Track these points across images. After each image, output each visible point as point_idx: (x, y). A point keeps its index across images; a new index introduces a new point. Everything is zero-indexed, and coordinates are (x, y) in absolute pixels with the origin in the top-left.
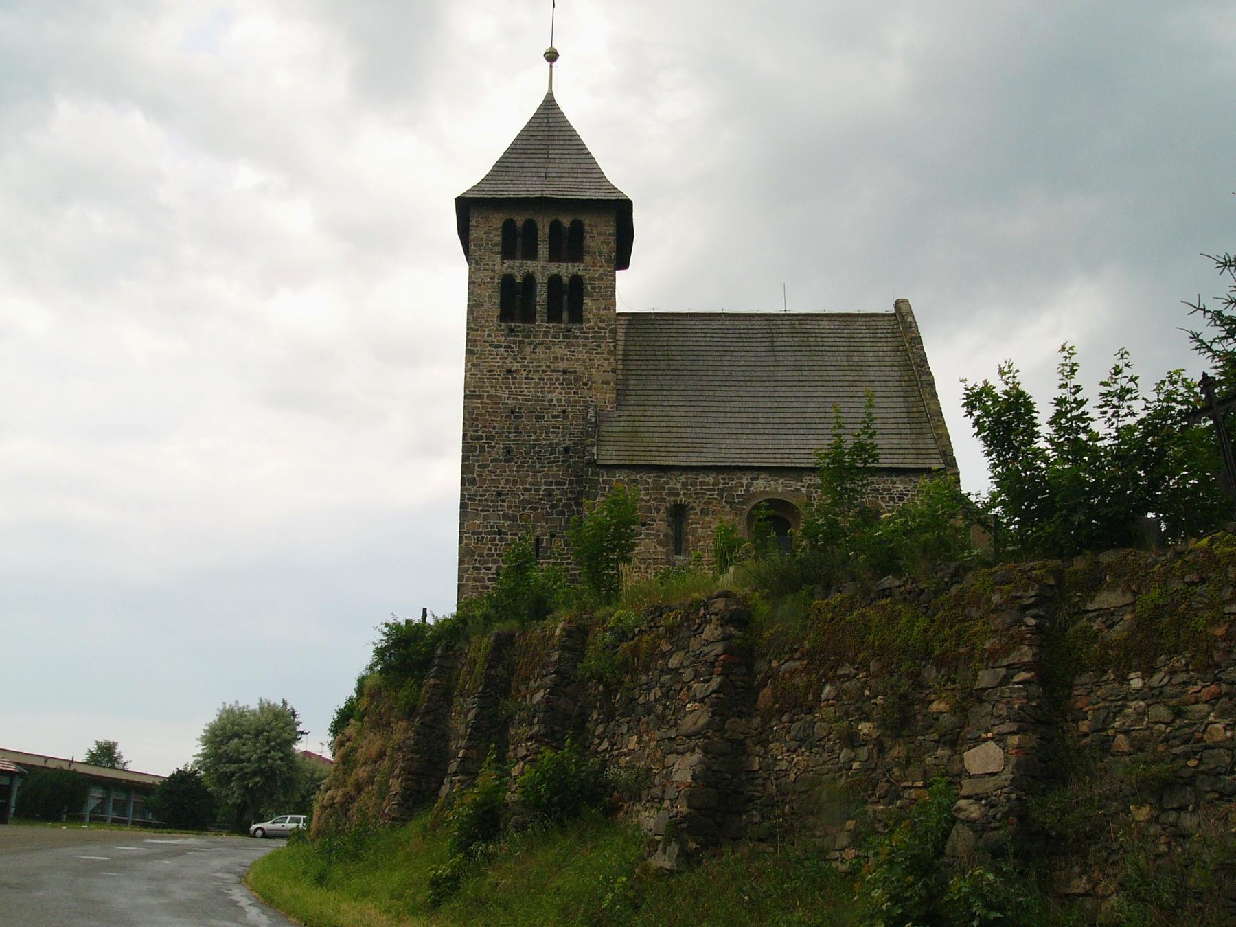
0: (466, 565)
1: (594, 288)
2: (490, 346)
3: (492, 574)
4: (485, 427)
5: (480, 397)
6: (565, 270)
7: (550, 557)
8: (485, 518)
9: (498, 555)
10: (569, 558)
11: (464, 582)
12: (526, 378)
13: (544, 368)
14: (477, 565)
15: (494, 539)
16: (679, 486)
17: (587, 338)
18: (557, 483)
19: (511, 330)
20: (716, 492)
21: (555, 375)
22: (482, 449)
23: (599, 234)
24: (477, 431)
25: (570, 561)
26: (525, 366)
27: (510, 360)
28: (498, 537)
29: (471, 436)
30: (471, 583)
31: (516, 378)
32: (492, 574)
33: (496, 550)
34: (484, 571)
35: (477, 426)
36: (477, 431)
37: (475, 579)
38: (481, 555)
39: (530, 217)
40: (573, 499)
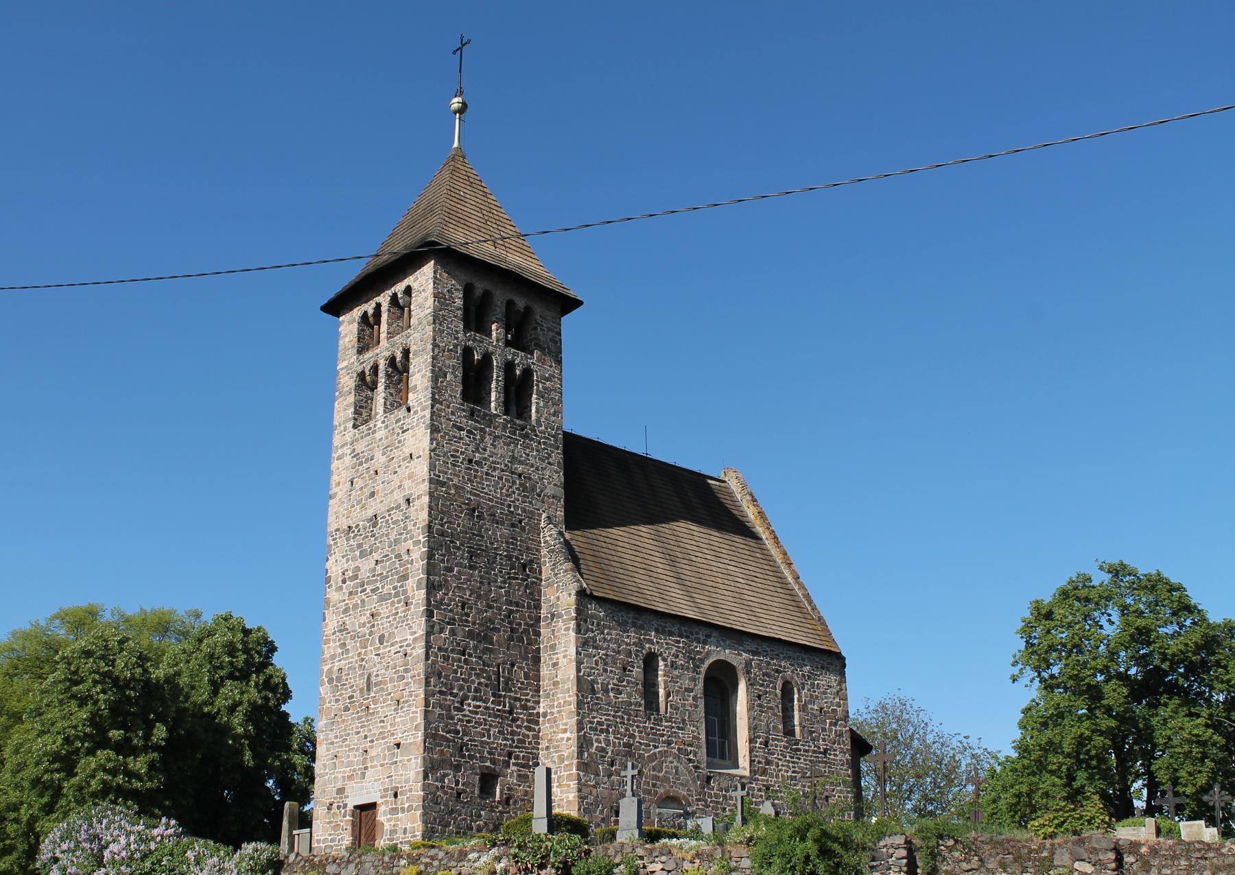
0: (432, 688)
4: (450, 522)
5: (443, 484)
6: (519, 358)
7: (510, 691)
8: (453, 632)
10: (528, 694)
11: (430, 708)
12: (487, 474)
13: (503, 466)
15: (459, 660)
17: (539, 443)
19: (472, 414)
20: (681, 645)
22: (448, 550)
23: (549, 329)
24: (442, 525)
26: (485, 459)
27: (470, 448)
28: (463, 658)
29: (437, 529)
30: (438, 711)
31: (477, 471)
32: (458, 702)
33: (461, 675)
35: (442, 520)
36: (442, 525)
37: (441, 706)
38: (447, 677)
39: (489, 289)
40: (532, 626)
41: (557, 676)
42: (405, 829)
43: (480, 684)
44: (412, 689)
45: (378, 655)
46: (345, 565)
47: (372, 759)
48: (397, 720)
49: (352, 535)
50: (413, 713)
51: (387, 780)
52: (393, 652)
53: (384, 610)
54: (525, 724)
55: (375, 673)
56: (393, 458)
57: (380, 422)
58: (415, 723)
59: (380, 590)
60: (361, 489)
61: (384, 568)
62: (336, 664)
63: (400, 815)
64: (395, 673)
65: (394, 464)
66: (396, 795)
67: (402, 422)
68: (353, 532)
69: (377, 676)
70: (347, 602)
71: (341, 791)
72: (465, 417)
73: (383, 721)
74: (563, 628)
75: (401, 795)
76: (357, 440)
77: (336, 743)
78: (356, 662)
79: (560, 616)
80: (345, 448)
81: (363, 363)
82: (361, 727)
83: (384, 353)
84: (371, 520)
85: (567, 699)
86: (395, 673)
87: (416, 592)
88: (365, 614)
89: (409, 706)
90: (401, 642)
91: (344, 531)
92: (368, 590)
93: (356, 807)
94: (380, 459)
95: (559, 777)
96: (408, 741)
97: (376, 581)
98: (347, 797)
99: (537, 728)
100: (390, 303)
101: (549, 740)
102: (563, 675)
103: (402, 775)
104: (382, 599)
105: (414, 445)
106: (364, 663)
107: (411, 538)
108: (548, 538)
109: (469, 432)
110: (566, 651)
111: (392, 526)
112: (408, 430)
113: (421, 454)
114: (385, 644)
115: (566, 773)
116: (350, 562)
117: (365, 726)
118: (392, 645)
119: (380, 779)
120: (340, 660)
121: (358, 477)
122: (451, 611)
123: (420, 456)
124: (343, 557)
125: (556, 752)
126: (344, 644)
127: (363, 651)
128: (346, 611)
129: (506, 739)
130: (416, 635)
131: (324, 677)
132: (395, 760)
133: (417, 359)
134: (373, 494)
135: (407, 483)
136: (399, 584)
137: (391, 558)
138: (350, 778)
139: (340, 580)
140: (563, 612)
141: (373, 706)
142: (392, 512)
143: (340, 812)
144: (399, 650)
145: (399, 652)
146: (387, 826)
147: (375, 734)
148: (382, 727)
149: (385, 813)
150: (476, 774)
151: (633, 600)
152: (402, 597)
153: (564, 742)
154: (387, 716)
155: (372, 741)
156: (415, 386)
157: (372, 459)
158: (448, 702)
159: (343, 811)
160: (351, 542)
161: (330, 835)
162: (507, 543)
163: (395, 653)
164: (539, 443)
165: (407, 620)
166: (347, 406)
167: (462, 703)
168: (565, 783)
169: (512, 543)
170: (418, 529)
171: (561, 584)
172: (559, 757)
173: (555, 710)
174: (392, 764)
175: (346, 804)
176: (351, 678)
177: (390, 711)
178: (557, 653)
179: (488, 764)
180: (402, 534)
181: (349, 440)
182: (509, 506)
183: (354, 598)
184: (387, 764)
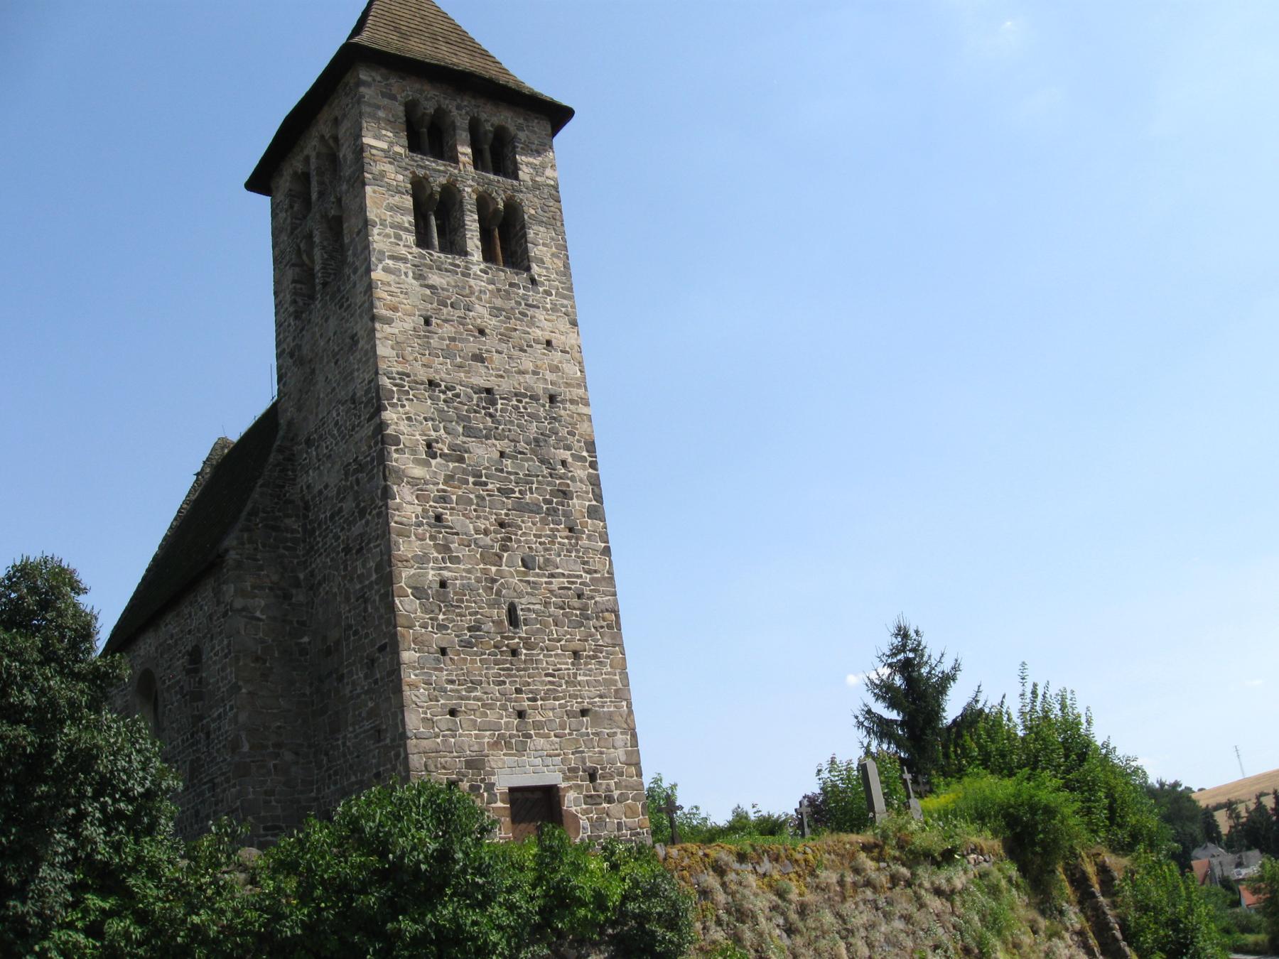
44: (601, 642)
45: (528, 582)
51: (573, 757)
52: (555, 587)
56: (516, 330)
59: (517, 495)
66: (592, 777)
70: (441, 486)
73: (553, 676)
75: (603, 777)
90: (570, 576)
92: (490, 487)
93: (512, 790)
96: (605, 709)
98: (493, 774)
104: (521, 507)
112: (538, 308)
118: (552, 576)
120: (441, 569)
126: (445, 548)
128: (444, 499)
130: (595, 575)
132: (584, 730)
136: (555, 500)
138: (495, 745)
141: (524, 651)
142: (524, 400)
144: (566, 585)
146: (584, 821)
148: (551, 683)
154: (560, 670)
155: (534, 700)
163: (560, 588)
165: (578, 551)
175: (494, 784)
177: (567, 664)
183: (459, 488)
184: (570, 734)
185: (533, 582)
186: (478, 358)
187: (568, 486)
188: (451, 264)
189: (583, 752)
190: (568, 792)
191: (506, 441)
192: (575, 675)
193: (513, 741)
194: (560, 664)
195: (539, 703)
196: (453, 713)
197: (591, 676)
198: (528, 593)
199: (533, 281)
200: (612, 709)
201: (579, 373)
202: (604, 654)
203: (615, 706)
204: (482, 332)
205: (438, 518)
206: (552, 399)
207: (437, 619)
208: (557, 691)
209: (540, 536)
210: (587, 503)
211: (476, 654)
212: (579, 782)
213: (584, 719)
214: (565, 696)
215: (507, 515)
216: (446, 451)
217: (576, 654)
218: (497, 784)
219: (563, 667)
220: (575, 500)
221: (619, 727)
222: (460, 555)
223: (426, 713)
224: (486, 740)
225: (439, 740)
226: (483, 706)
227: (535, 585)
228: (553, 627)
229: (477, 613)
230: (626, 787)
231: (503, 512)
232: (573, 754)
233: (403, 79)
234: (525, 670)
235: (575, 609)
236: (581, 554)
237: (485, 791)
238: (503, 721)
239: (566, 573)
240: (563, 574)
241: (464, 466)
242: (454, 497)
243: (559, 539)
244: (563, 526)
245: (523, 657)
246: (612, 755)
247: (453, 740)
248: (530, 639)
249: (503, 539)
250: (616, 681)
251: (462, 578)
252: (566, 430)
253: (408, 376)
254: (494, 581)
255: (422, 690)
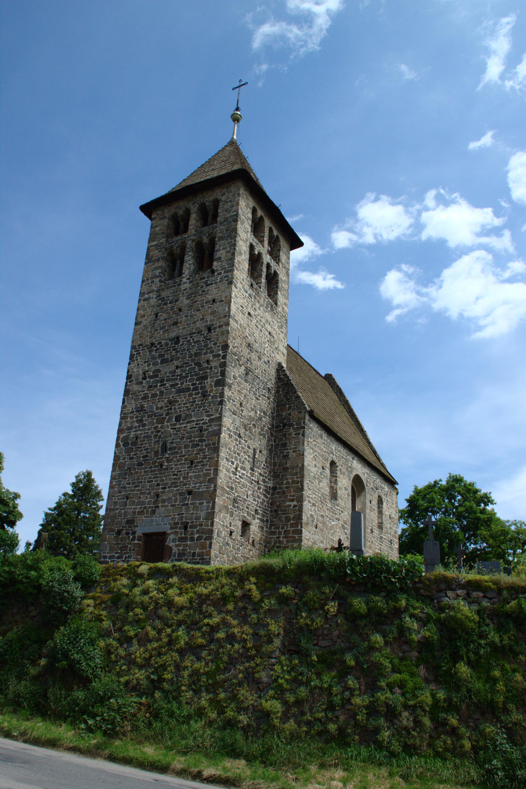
1: (282, 287)
2: (243, 288)
3: (234, 468)
4: (238, 347)
9: (238, 454)
14: (228, 457)
16: (333, 448)
18: (264, 412)
21: (267, 333)
25: (266, 475)
32: (234, 468)
34: (230, 463)
38: (230, 449)
41: (286, 464)
42: (194, 553)
43: (245, 458)
44: (207, 453)
45: (175, 429)
46: (147, 368)
47: (164, 501)
48: (190, 475)
49: (155, 349)
50: (206, 470)
51: (177, 517)
53: (182, 399)
54: (264, 493)
55: (170, 441)
56: (197, 301)
57: (185, 279)
58: (208, 478)
59: (179, 385)
60: (165, 320)
61: (184, 371)
62: (133, 433)
63: (189, 543)
64: (190, 442)
65: (198, 305)
66: (186, 528)
67: (206, 279)
68: (156, 346)
69: (172, 443)
70: (146, 392)
71: (130, 522)
72: (248, 285)
73: (176, 475)
74: (294, 433)
75: (191, 527)
76: (163, 290)
77: (128, 487)
78: (152, 432)
79: (292, 425)
80: (151, 294)
81: (171, 243)
82: (154, 478)
83: (192, 237)
84: (173, 339)
85: (295, 479)
86: (190, 442)
87: (214, 388)
88: (162, 401)
89: (203, 465)
90: (197, 421)
91: (147, 346)
92: (167, 385)
93: (145, 535)
94: (184, 301)
95: (285, 532)
96: (201, 490)
97: (177, 379)
98: (137, 526)
99: (269, 496)
100: (198, 209)
101: (278, 506)
102: (292, 463)
103: (192, 514)
104: (180, 391)
105: (217, 293)
106: (159, 434)
107: (211, 352)
108: (282, 376)
109: (249, 295)
110: (296, 448)
111: (193, 344)
112: (212, 284)
113: (223, 299)
114: (181, 422)
115: (292, 529)
116: (151, 366)
117: (158, 477)
119: (171, 516)
121: (163, 312)
122: (235, 405)
123: (223, 301)
124: (145, 362)
125: (283, 514)
126: (141, 421)
127: (160, 426)
128: (145, 397)
129: (255, 500)
131: (120, 442)
132: (186, 502)
133: (223, 241)
134: (176, 323)
135: (209, 318)
136: (198, 382)
137: (191, 365)
139: (141, 377)
140: (294, 423)
141: (166, 464)
142: (194, 336)
143: (129, 537)
144: (195, 426)
145: (196, 427)
146: (175, 550)
147: (168, 483)
148: (175, 479)
149: (174, 540)
150: (240, 521)
151: (328, 423)
152: (201, 391)
153: (292, 507)
154: (181, 471)
155: (165, 488)
156: (220, 258)
157: (177, 301)
158: (229, 467)
159: (131, 537)
160: (153, 353)
161: (117, 553)
162: (262, 372)
163: (190, 429)
164: (277, 316)
165: (204, 406)
166: (155, 268)
167: (236, 469)
168: (291, 535)
169: (264, 374)
170: (218, 347)
171: (292, 405)
172: (286, 517)
173: (284, 486)
174: (184, 505)
175: (136, 532)
176: (146, 444)
178: (288, 449)
179: (246, 515)
180: (203, 349)
181: (155, 289)
182: (264, 350)
183: (153, 390)
184: (178, 505)
185: (178, 428)
186: (176, 323)
187: (207, 372)
188: (173, 283)
189: (183, 514)
190: (170, 535)
191: (180, 360)
192: (188, 473)
193: (150, 510)
194: (181, 468)
195: (167, 489)
196: (127, 498)
197: (196, 472)
198: (174, 434)
199: (213, 272)
200: (205, 490)
201: (227, 309)
202: (207, 459)
203: (206, 488)
204: (180, 310)
205: (142, 407)
206: (209, 330)
207: (129, 455)
208: (177, 483)
209: (186, 404)
210: (215, 379)
211: (143, 469)
212: (178, 530)
213: (188, 497)
214: (181, 485)
215: (173, 397)
216: (151, 374)
217: (192, 462)
218: (138, 531)
219: (182, 470)
220: (209, 379)
221: (206, 499)
222: (146, 422)
223: (115, 499)
224: (137, 510)
225: (117, 512)
226: (140, 494)
227: (179, 430)
228: (183, 450)
229: (148, 449)
230: (202, 533)
231: (171, 396)
232: (178, 515)
233: (170, 206)
234: (164, 473)
235: (196, 438)
236: (206, 408)
237: (132, 535)
238: (147, 501)
239: (195, 419)
240: (193, 421)
241: (158, 379)
242: (150, 396)
243: (197, 402)
244: (200, 395)
245: (164, 467)
246: (199, 515)
247: (123, 511)
248: (169, 457)
249: (168, 410)
250: (210, 474)
251: (145, 433)
252: (213, 343)
253: (141, 345)
254: (159, 431)
255: (116, 489)
